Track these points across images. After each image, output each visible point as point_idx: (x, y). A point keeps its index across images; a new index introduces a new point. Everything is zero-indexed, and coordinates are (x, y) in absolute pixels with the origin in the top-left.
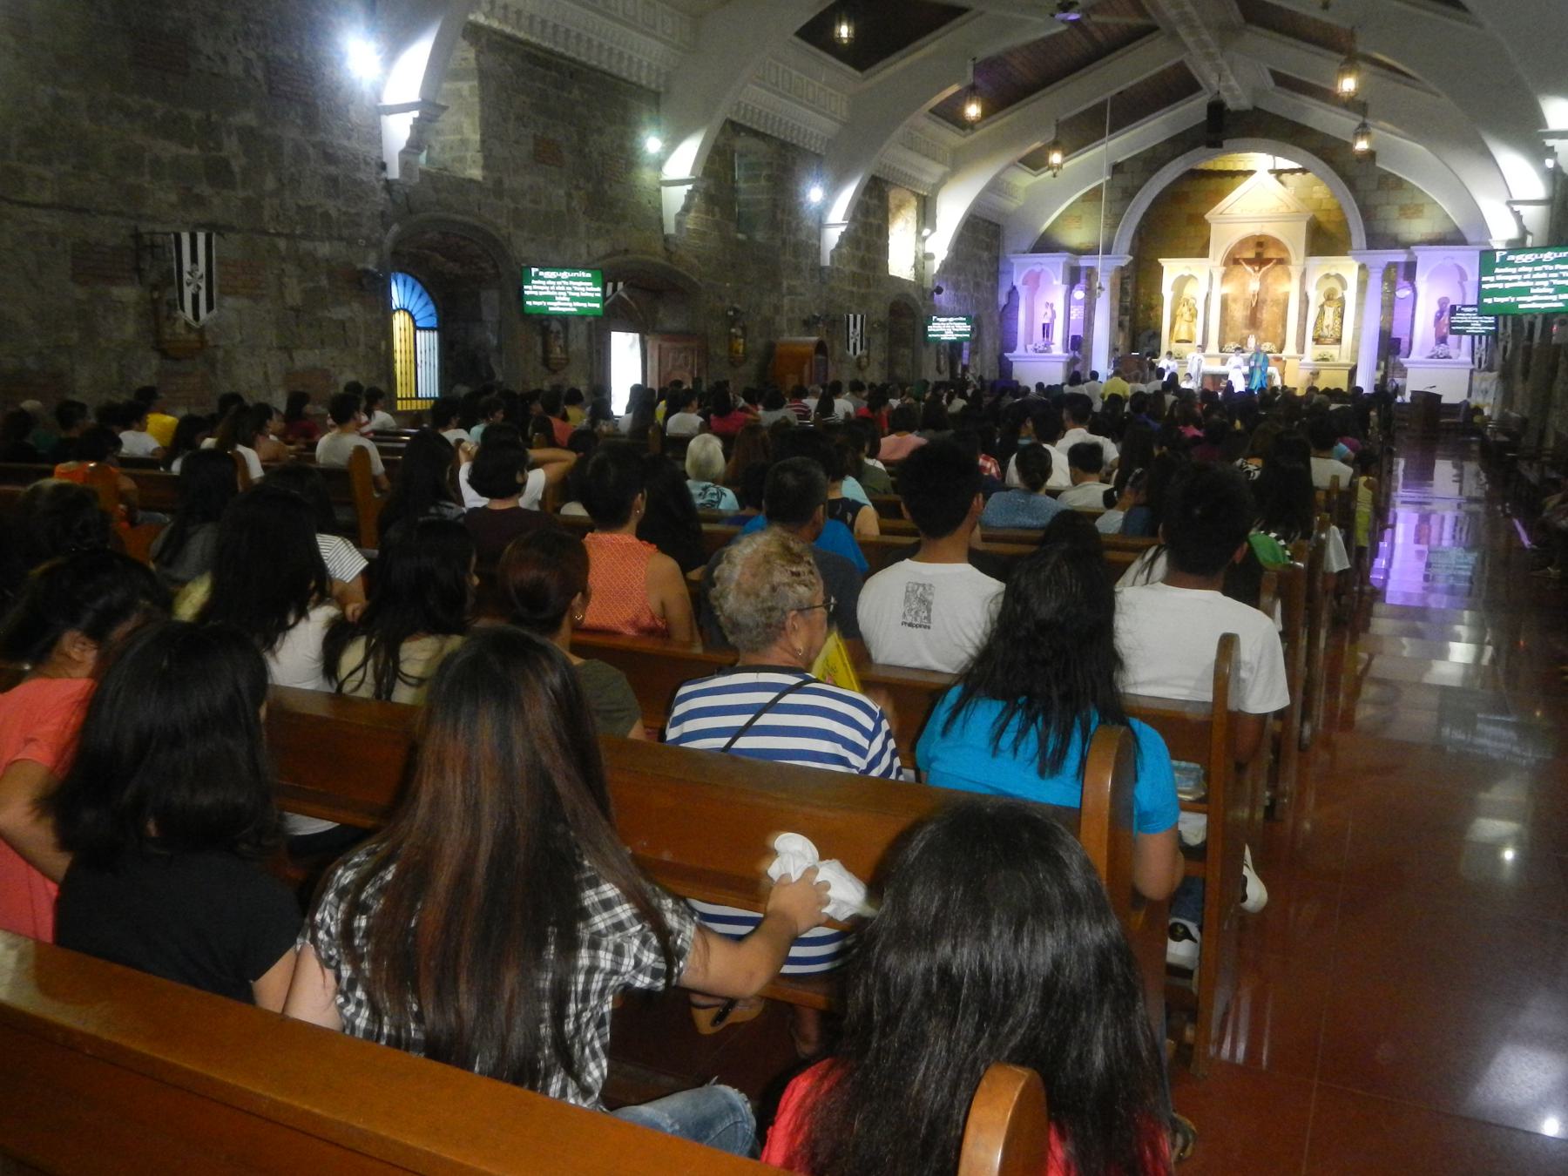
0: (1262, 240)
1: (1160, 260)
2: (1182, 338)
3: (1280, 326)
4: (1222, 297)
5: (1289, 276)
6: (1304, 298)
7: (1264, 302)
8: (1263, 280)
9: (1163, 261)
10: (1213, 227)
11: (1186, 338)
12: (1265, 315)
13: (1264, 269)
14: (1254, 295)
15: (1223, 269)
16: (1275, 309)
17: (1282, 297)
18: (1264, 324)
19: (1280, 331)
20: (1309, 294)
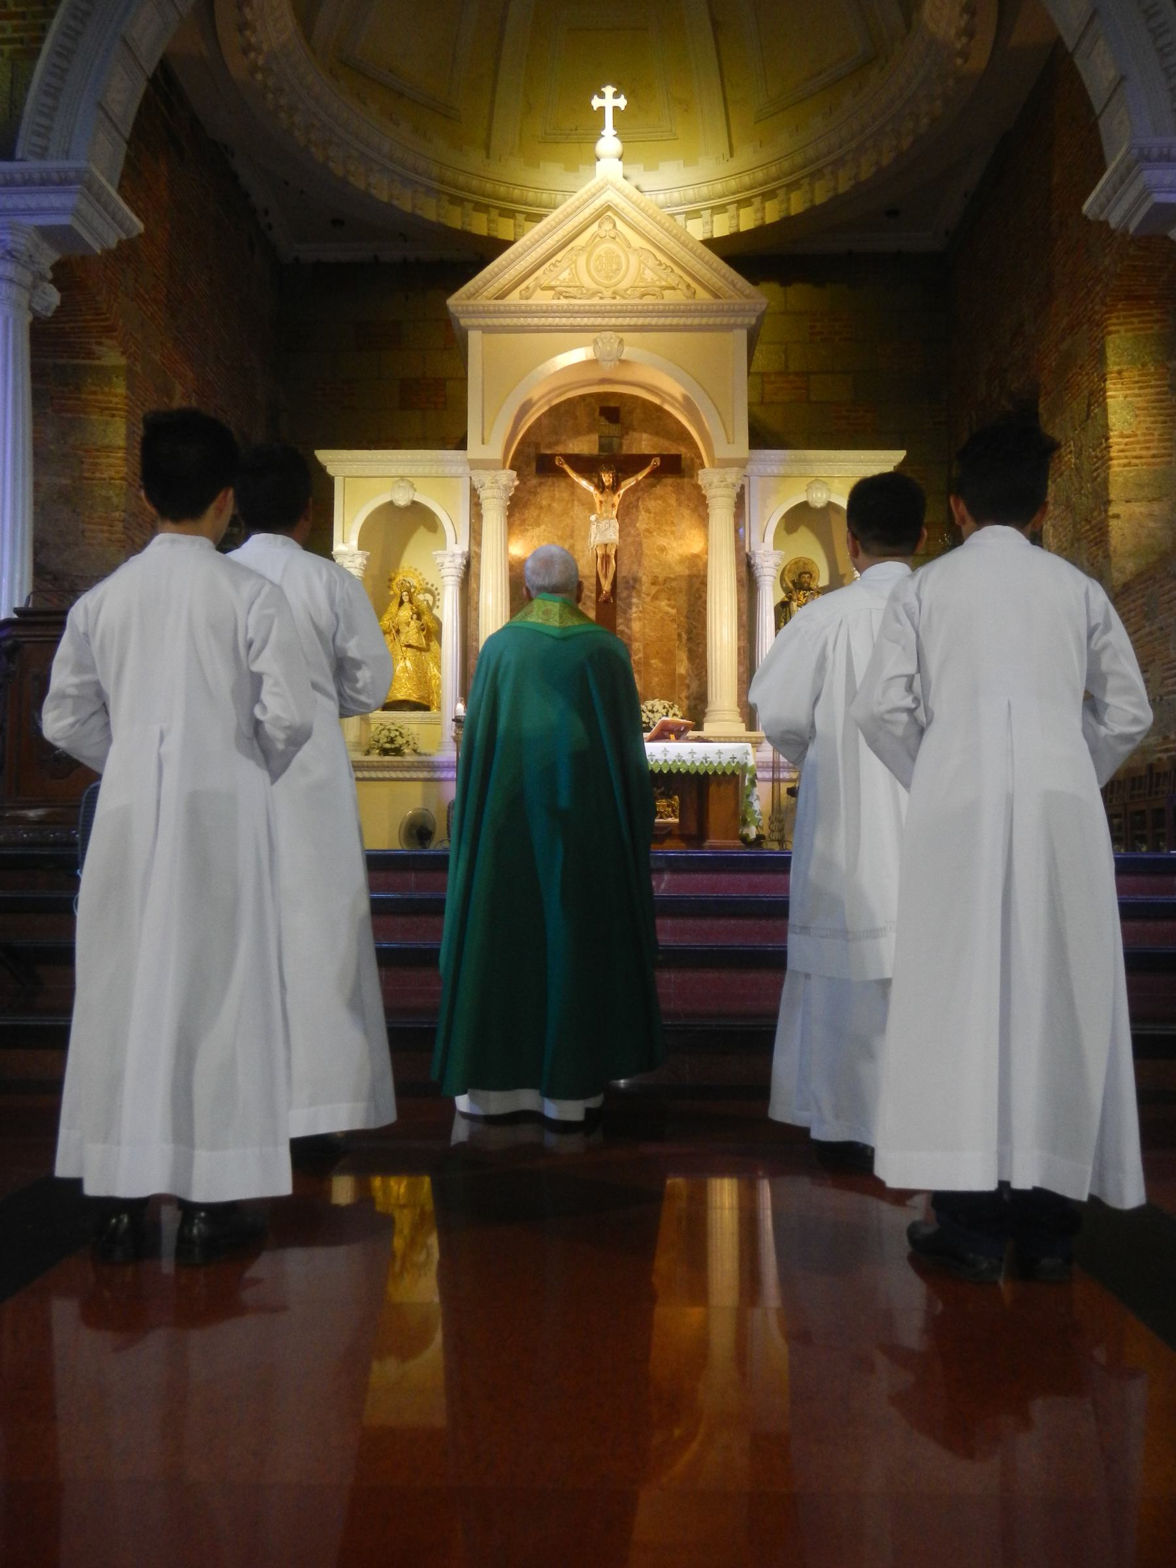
0: (612, 404)
1: (322, 455)
2: (401, 695)
3: (682, 655)
4: (512, 568)
5: (700, 506)
6: (744, 575)
7: (633, 584)
8: (626, 514)
9: (334, 461)
10: (476, 341)
11: (414, 698)
12: (636, 626)
13: (630, 483)
14: (606, 558)
15: (508, 478)
16: (663, 604)
17: (683, 570)
18: (636, 646)
19: (682, 668)
20: (757, 560)
